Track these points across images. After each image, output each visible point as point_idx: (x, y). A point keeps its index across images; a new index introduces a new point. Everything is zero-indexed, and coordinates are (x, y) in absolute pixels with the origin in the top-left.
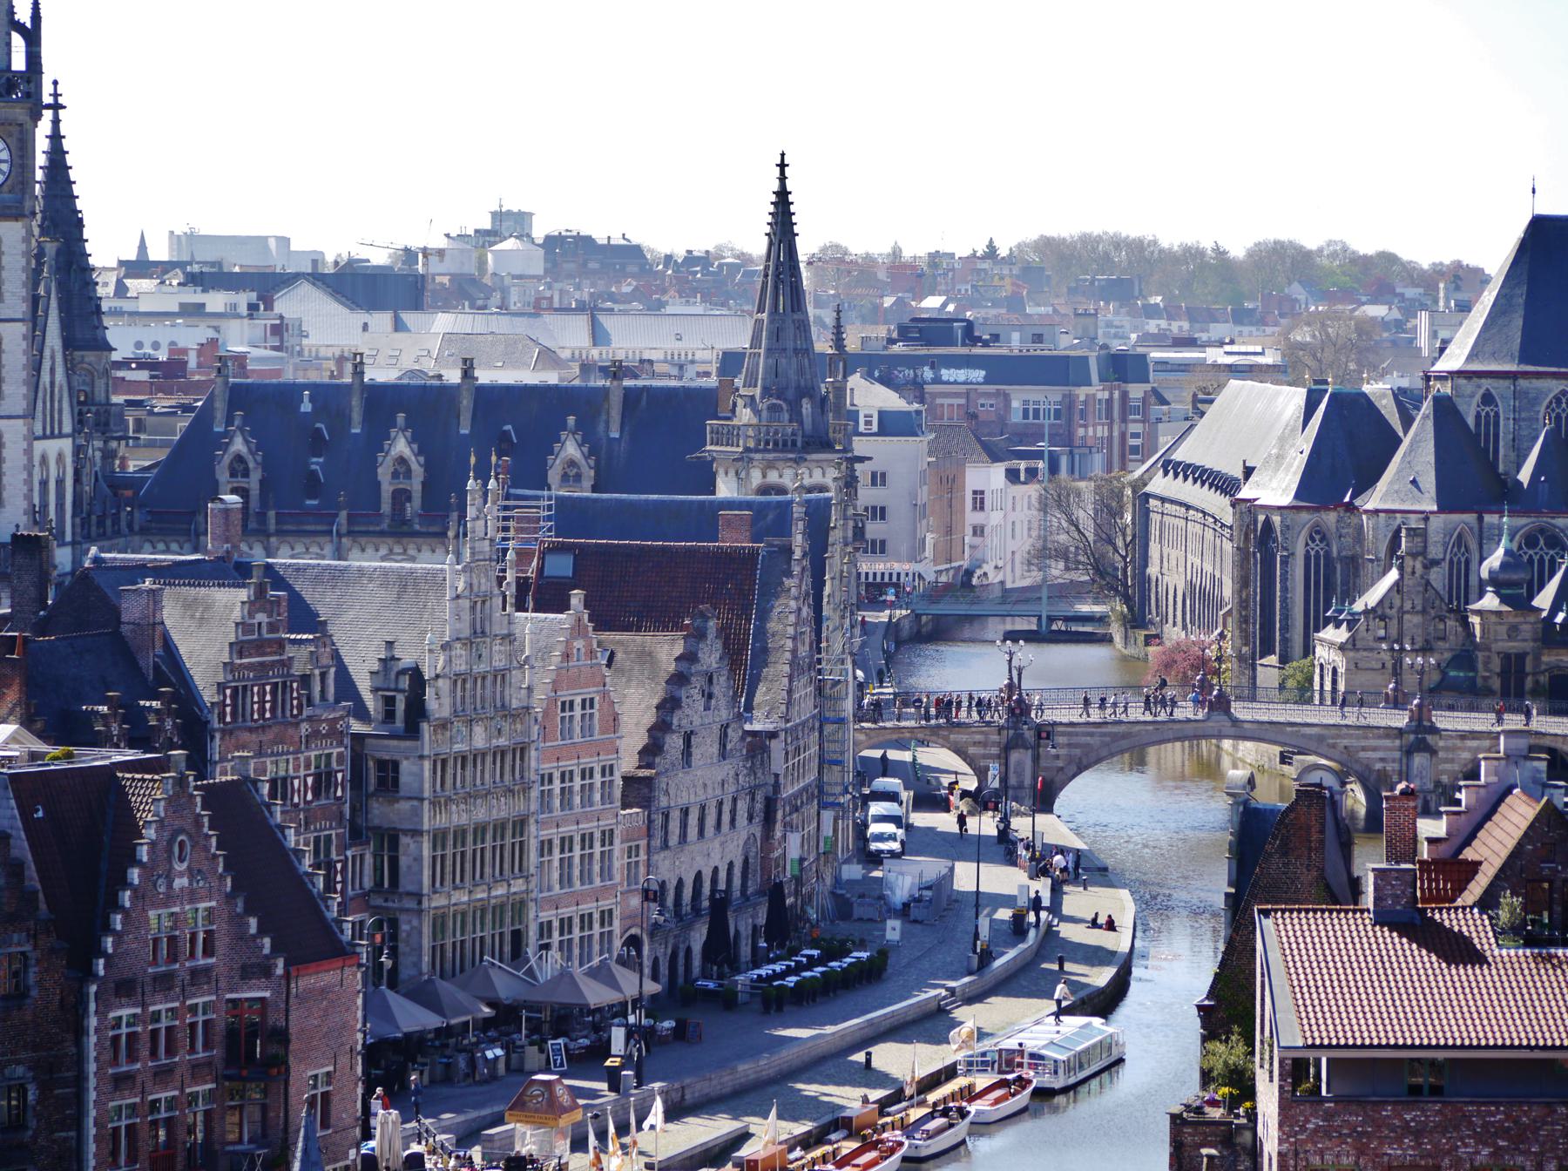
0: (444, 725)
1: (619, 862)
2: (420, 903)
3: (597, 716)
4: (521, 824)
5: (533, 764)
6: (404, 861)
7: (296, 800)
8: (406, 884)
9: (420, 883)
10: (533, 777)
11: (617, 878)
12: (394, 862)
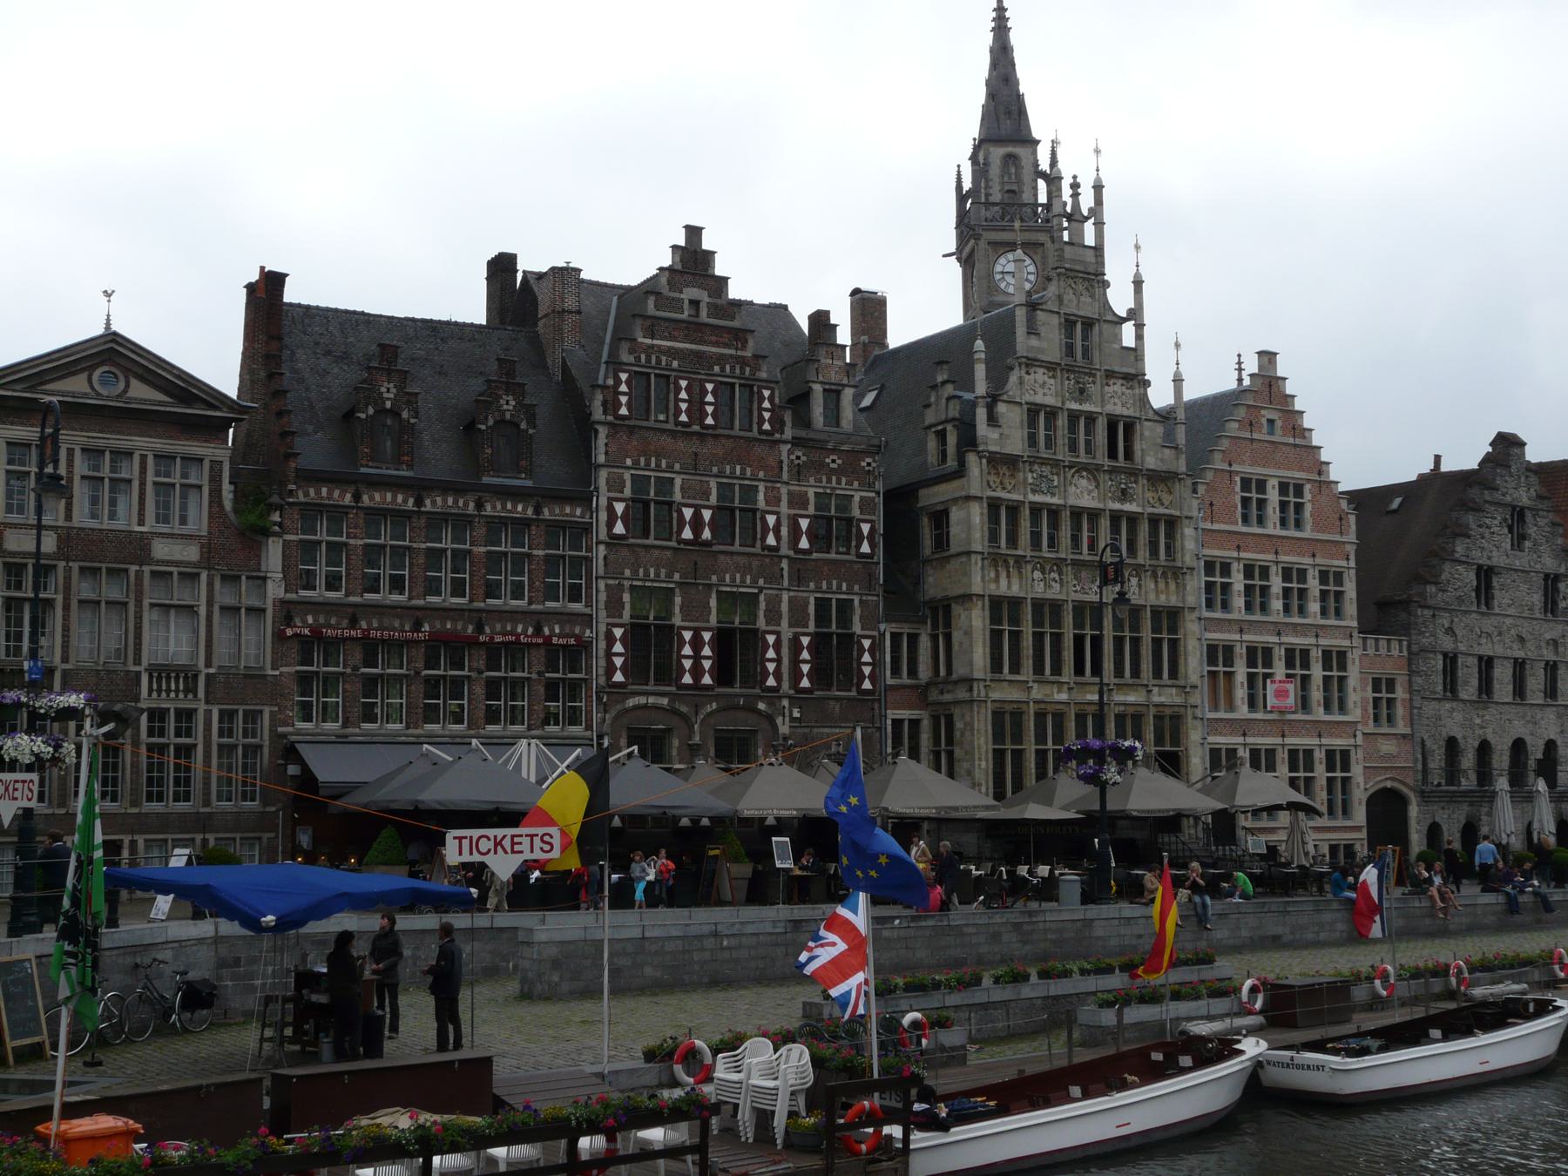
0: (1012, 462)
1: (1358, 694)
2: (971, 690)
3: (1308, 508)
4: (1169, 618)
5: (1190, 545)
6: (957, 636)
7: (771, 540)
8: (960, 670)
9: (971, 663)
10: (1189, 560)
11: (1355, 714)
12: (948, 637)
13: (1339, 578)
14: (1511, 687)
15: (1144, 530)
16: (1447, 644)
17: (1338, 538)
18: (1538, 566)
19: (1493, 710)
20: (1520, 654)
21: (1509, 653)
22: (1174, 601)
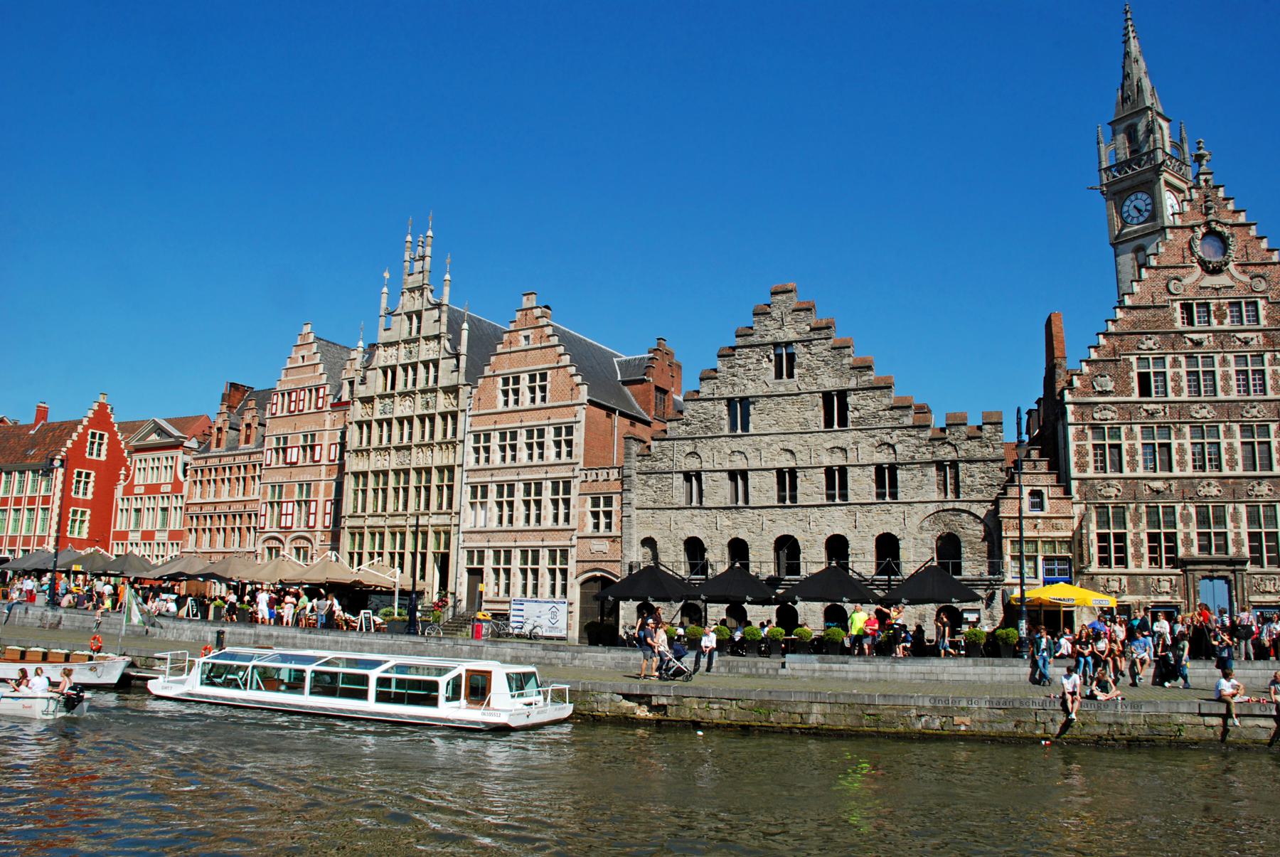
1: (581, 508)
11: (574, 523)
13: (570, 431)
14: (774, 493)
15: (438, 420)
16: (693, 464)
17: (569, 402)
18: (814, 388)
19: (749, 513)
20: (785, 462)
21: (770, 465)
22: (451, 462)
